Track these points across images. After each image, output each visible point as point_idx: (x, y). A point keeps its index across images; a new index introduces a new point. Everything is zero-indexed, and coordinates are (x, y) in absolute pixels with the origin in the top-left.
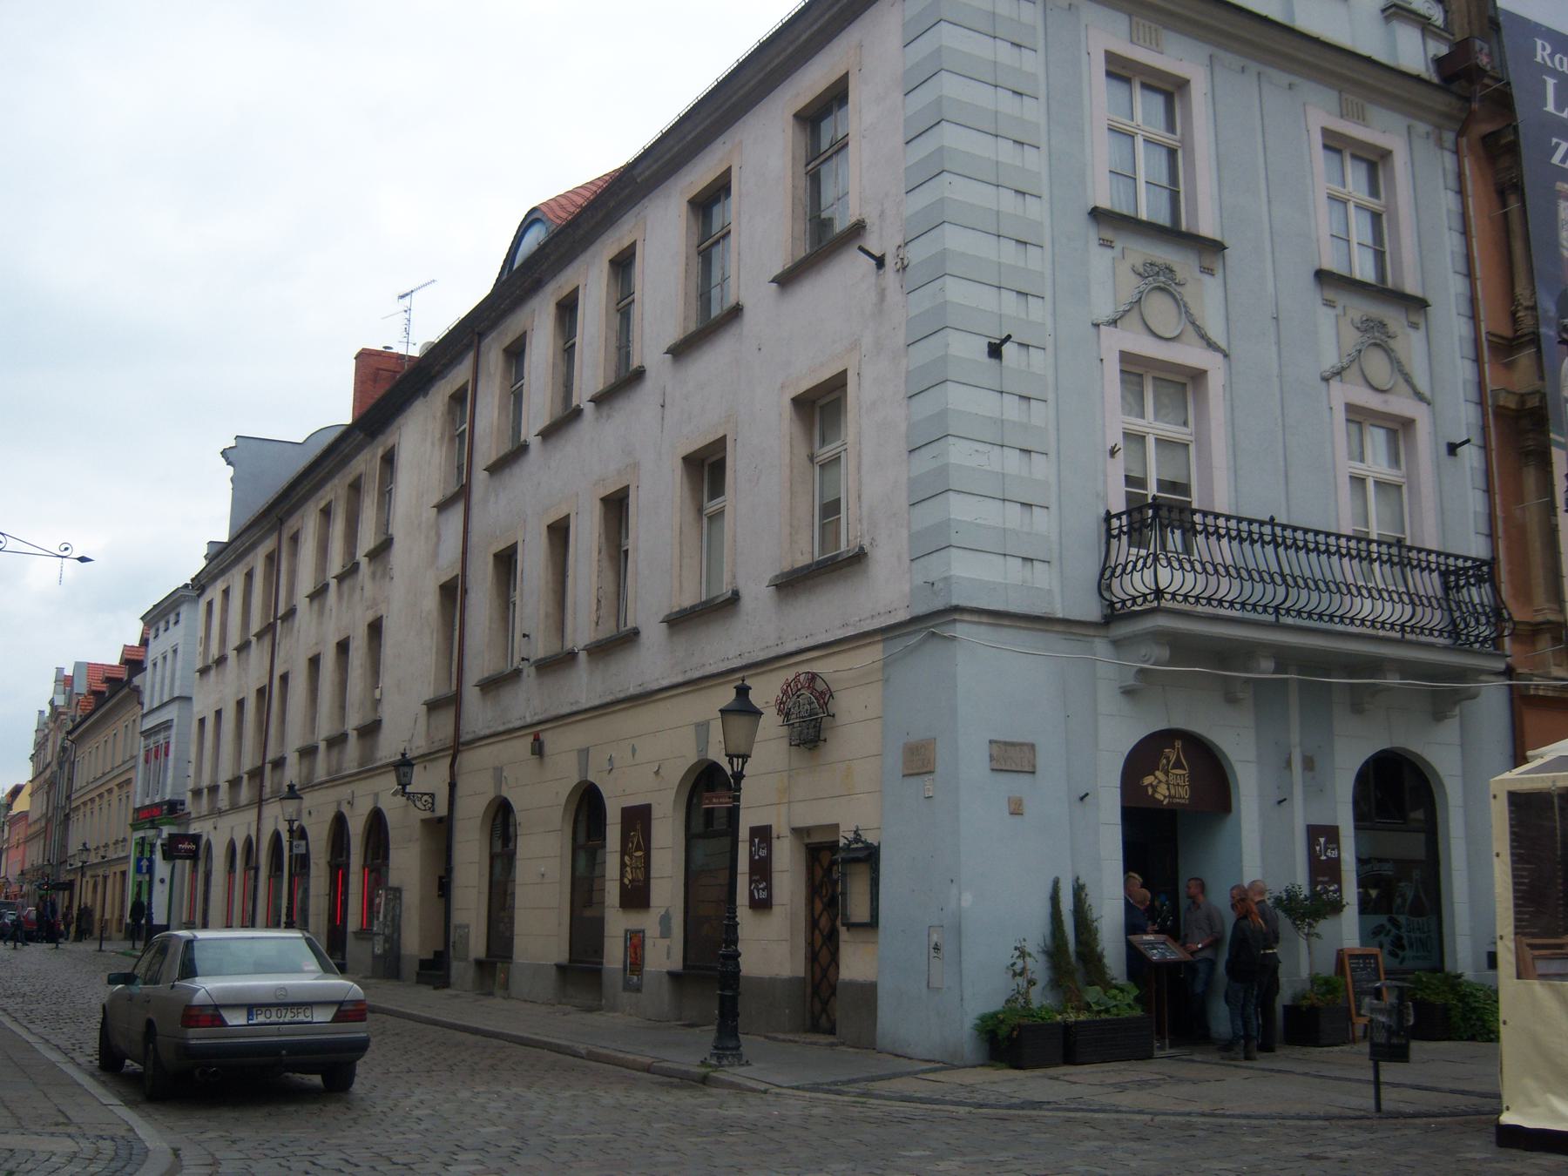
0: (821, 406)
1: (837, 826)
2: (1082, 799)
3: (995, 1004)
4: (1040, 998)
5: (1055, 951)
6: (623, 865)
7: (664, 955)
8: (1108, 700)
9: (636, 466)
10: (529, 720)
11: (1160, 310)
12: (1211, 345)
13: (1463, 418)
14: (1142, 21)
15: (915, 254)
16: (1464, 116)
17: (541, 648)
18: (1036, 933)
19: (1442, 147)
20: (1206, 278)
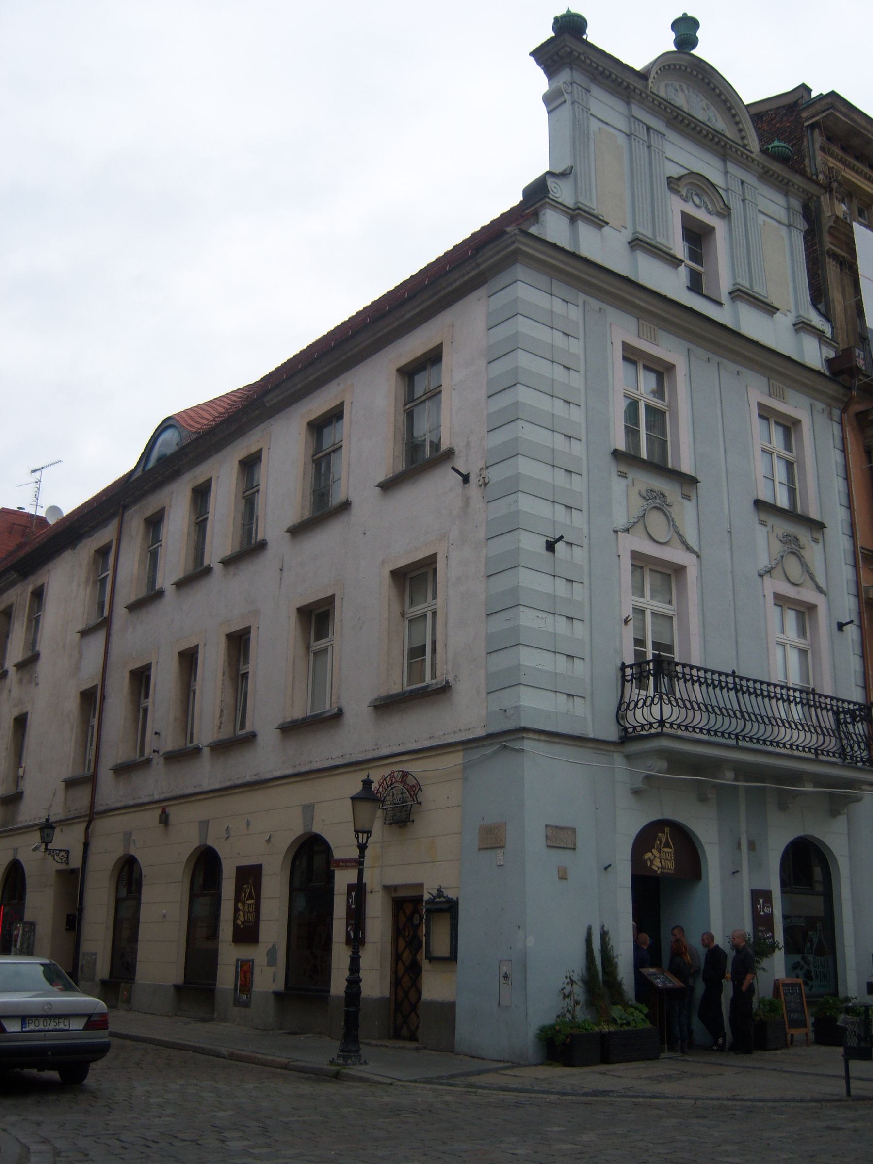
0: (414, 578)
1: (421, 886)
2: (606, 868)
3: (549, 1019)
4: (582, 1015)
5: (590, 980)
6: (236, 910)
7: (269, 978)
11: (657, 523)
12: (689, 549)
13: (846, 605)
14: (645, 323)
15: (495, 475)
16: (846, 400)
18: (576, 964)
19: (831, 419)
20: (686, 502)
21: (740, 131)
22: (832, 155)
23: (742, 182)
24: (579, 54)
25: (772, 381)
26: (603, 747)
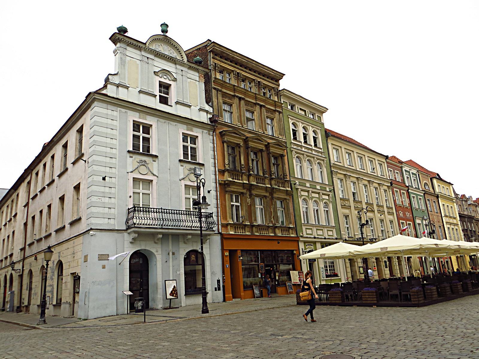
8: (127, 244)
9: (52, 199)
10: (35, 252)
11: (143, 169)
12: (154, 175)
14: (142, 114)
15: (90, 160)
17: (37, 238)
21: (182, 56)
22: (216, 59)
23: (182, 70)
24: (122, 39)
25: (188, 126)
26: (119, 231)
